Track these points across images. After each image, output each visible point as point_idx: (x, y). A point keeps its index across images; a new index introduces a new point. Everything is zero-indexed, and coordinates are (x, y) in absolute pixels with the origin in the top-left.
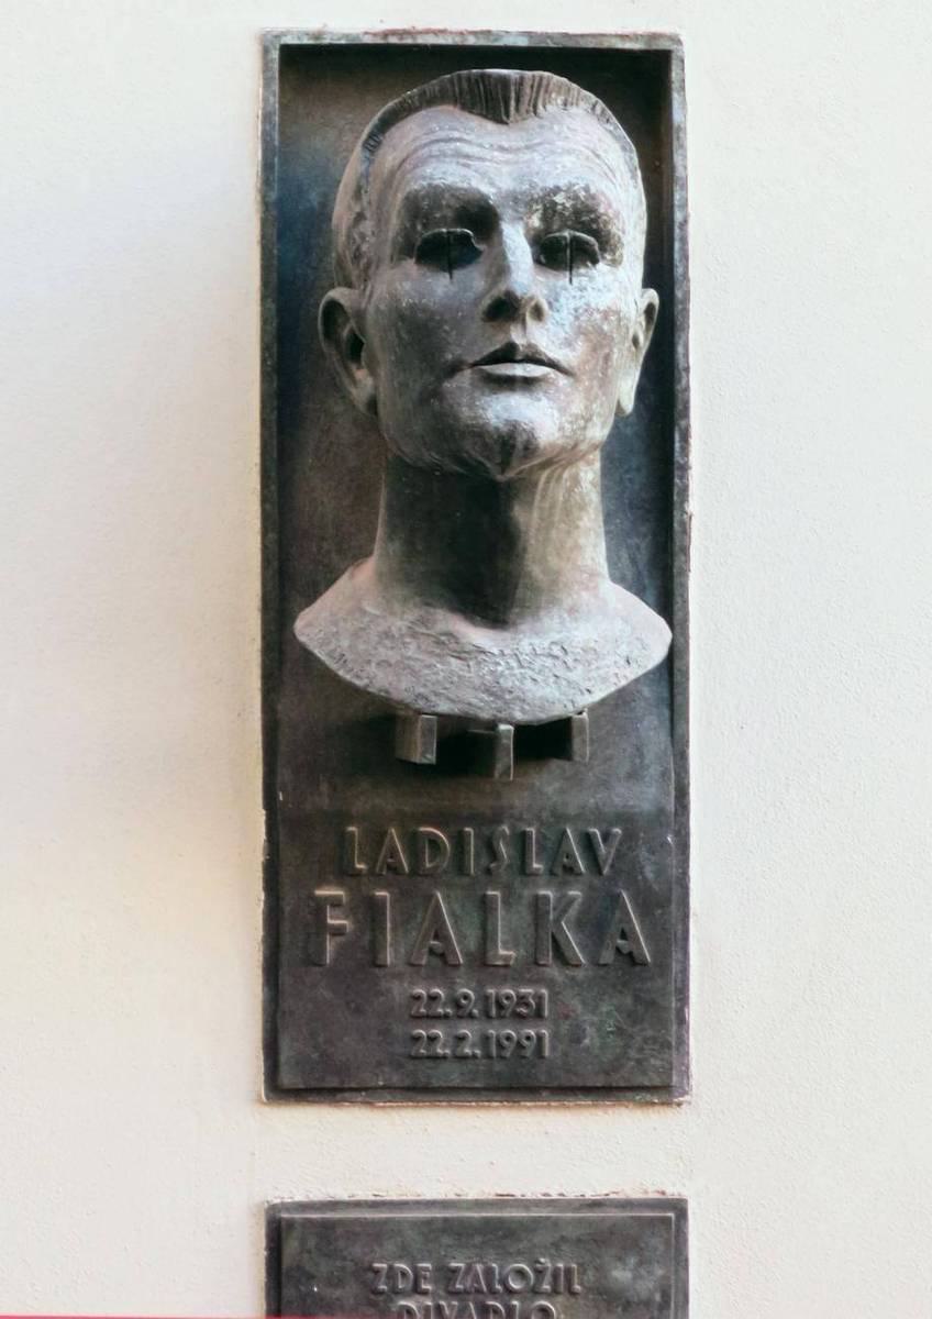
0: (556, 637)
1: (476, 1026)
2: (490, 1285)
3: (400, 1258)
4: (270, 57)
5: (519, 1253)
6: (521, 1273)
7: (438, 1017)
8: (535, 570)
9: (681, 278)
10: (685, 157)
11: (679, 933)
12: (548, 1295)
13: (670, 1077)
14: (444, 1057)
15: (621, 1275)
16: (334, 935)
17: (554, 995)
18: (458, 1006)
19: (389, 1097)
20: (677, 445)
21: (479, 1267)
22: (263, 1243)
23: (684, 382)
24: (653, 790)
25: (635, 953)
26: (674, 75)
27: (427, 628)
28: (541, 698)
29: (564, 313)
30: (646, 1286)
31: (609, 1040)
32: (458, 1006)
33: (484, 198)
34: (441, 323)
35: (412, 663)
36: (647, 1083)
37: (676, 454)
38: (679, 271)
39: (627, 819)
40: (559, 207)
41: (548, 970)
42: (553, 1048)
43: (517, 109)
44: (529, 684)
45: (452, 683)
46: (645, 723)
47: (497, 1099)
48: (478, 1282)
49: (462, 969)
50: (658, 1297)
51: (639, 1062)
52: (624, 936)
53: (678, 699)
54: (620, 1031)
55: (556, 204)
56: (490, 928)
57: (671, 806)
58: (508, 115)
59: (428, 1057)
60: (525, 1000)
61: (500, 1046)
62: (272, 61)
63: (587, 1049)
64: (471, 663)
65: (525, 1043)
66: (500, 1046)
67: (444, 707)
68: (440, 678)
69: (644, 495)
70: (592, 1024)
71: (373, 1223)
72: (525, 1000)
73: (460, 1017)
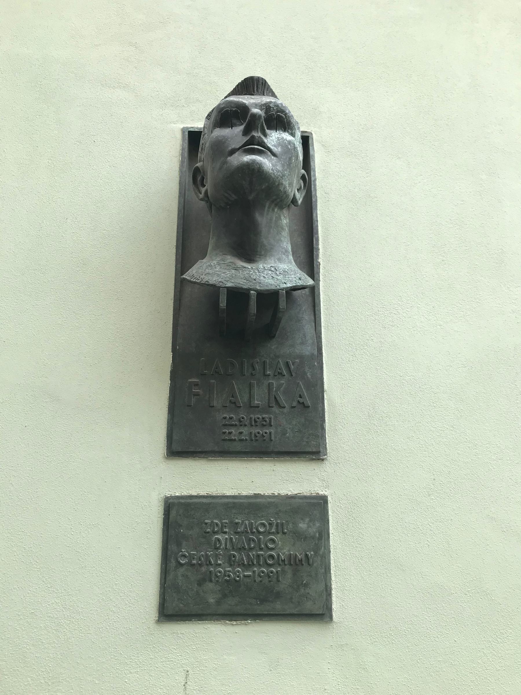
0: (273, 265)
1: (246, 428)
2: (251, 529)
3: (216, 518)
4: (185, 134)
5: (262, 516)
6: (263, 525)
7: (232, 425)
8: (265, 242)
9: (314, 195)
10: (314, 163)
11: (320, 397)
12: (273, 533)
13: (319, 448)
14: (235, 440)
15: (303, 526)
16: (194, 395)
17: (276, 417)
18: (240, 421)
19: (213, 455)
20: (314, 242)
21: (247, 522)
22: (162, 512)
23: (316, 224)
24: (310, 348)
25: (305, 403)
26: (310, 142)
27: (224, 261)
28: (267, 282)
29: (274, 138)
30: (313, 530)
31: (296, 434)
32: (240, 421)
33: (245, 104)
34: (227, 139)
35: (217, 272)
36: (310, 450)
37: (314, 245)
38: (313, 193)
39: (301, 357)
40: (272, 109)
41: (273, 409)
42: (275, 437)
43: (257, 91)
44: (262, 278)
45: (233, 277)
46: (306, 327)
47: (254, 456)
48: (246, 528)
49: (242, 408)
50: (317, 535)
51: (307, 442)
52: (300, 397)
53: (317, 319)
54: (300, 431)
55: (271, 107)
56: (252, 393)
57: (316, 353)
58: (254, 92)
59: (229, 440)
60: (265, 419)
61: (256, 436)
62: (186, 135)
63: (288, 438)
64: (240, 271)
65: (265, 434)
66: (256, 436)
67: (229, 285)
68: (228, 276)
69: (303, 261)
70: (289, 428)
71: (205, 504)
72: (265, 419)
73: (241, 425)
